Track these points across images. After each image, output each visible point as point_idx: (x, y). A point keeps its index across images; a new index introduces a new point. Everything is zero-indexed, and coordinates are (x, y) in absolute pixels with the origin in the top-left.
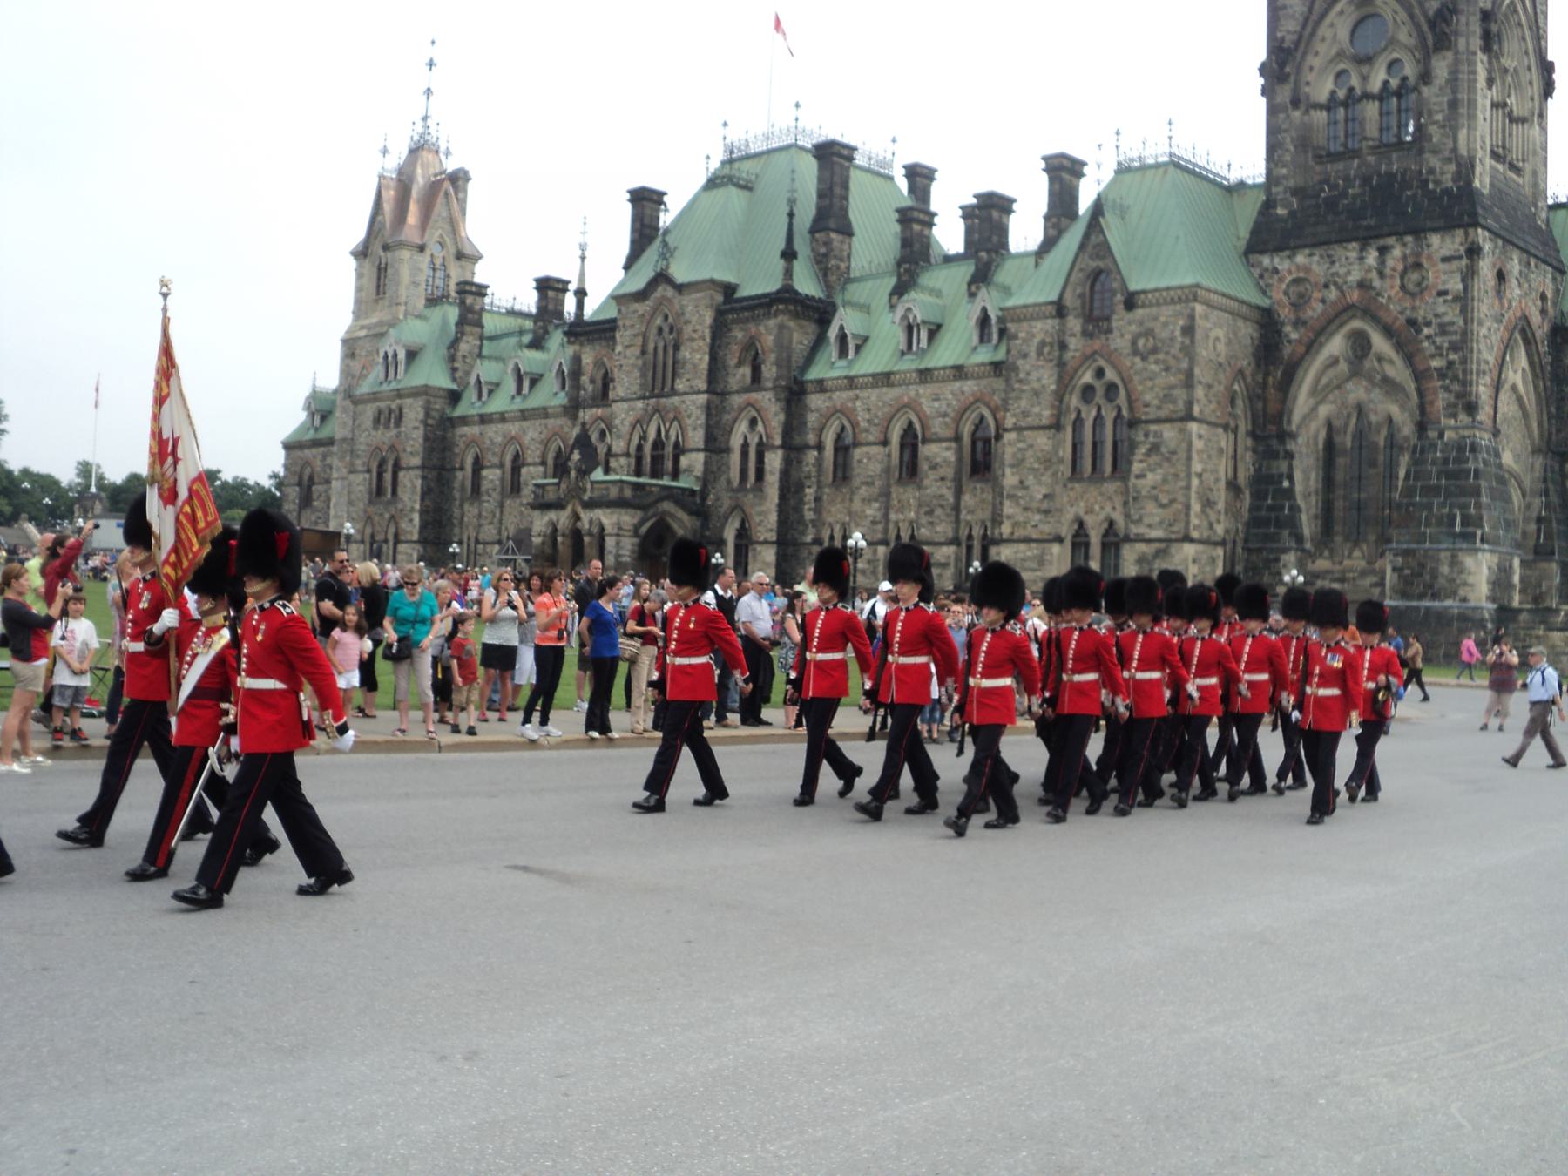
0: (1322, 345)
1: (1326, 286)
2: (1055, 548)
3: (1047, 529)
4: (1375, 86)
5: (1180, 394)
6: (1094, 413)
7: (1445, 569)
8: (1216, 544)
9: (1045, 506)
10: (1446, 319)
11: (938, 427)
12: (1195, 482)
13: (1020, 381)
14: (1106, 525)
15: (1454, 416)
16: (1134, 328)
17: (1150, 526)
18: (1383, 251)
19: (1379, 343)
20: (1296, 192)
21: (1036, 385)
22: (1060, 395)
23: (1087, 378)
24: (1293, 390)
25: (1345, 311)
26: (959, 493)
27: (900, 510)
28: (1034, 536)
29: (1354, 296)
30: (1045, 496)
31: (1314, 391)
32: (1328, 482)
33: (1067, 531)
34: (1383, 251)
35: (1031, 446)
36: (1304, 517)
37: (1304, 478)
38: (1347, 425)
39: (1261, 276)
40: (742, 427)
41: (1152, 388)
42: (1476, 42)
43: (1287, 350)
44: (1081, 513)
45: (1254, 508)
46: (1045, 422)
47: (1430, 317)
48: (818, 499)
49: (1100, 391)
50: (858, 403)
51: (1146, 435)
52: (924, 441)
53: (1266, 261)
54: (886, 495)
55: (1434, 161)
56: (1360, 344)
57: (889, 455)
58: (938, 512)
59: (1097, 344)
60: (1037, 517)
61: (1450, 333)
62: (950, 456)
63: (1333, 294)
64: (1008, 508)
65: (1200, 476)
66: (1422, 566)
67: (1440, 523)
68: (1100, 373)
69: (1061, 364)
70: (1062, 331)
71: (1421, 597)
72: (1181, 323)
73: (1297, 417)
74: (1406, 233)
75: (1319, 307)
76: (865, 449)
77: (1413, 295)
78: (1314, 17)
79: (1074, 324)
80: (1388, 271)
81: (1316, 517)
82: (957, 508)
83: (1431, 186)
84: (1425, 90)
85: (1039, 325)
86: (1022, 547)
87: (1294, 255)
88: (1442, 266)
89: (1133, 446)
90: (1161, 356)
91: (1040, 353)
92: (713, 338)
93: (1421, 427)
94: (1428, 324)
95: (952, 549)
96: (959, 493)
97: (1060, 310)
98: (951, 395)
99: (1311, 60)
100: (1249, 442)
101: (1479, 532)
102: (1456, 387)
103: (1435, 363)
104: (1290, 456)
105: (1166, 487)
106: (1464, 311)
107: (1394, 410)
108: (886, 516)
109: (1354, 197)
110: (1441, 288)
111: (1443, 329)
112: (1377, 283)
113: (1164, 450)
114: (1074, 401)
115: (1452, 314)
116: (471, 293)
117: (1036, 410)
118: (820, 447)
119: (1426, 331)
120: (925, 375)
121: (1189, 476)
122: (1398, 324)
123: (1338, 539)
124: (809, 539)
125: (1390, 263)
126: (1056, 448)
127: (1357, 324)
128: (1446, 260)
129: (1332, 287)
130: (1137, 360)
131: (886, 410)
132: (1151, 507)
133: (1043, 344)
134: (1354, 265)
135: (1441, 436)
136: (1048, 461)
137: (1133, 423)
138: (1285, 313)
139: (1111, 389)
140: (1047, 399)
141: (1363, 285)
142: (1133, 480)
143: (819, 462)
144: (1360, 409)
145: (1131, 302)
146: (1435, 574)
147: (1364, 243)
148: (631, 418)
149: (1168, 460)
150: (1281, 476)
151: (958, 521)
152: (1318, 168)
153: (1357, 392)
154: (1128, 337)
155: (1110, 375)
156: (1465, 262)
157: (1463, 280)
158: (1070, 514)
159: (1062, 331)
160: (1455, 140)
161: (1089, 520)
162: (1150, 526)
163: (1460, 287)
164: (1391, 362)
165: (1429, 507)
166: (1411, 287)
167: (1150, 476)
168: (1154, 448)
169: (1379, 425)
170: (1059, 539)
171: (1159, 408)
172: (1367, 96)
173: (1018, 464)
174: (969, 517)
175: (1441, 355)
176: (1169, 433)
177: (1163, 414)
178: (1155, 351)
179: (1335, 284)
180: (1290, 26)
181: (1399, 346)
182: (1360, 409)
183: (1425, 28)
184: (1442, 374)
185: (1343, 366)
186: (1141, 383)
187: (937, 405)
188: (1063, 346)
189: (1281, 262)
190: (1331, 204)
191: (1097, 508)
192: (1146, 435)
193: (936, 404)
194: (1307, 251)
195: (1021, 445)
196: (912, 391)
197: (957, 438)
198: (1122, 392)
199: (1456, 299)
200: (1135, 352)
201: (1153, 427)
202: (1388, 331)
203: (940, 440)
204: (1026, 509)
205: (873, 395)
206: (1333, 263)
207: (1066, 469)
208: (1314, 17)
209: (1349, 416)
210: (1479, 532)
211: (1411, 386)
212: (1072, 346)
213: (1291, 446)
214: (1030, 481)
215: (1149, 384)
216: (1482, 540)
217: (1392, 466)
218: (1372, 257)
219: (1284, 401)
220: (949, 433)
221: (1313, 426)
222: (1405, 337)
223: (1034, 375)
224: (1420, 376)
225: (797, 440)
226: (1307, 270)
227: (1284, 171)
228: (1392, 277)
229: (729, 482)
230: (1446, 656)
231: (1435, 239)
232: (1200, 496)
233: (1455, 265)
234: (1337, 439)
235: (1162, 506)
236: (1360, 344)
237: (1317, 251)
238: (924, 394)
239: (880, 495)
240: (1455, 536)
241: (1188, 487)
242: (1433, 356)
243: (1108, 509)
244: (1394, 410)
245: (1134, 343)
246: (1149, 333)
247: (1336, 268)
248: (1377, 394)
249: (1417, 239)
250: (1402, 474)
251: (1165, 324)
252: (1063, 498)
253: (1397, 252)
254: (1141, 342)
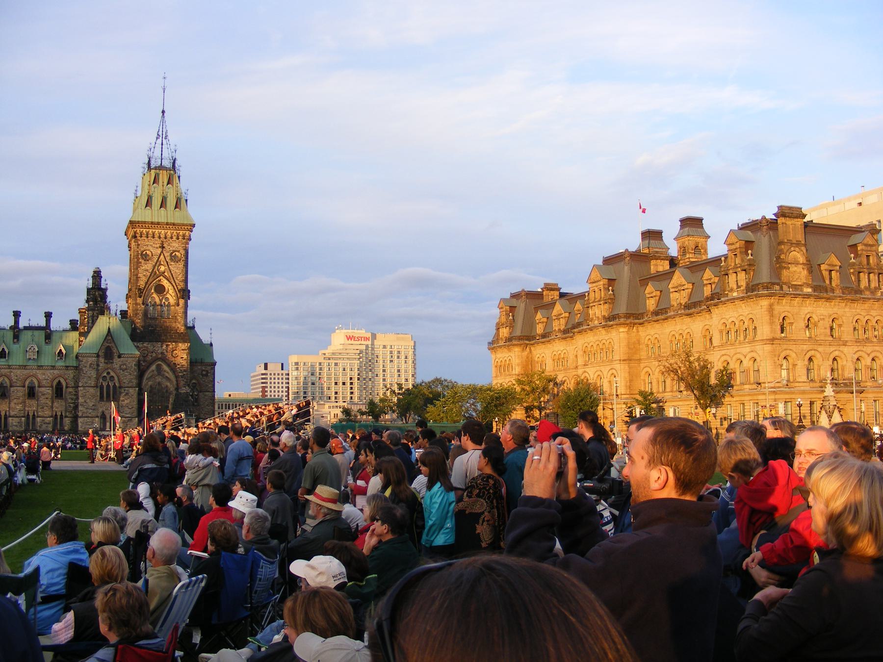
3: (94, 414)
11: (44, 383)
18: (167, 345)
19: (165, 367)
22: (97, 379)
25: (157, 359)
26: (53, 403)
27: (30, 406)
34: (167, 345)
52: (39, 387)
56: (159, 366)
59: (109, 366)
63: (154, 355)
64: (80, 408)
68: (108, 373)
69: (97, 370)
70: (98, 361)
79: (102, 360)
82: (52, 407)
89: (121, 393)
93: (177, 389)
96: (53, 403)
97: (98, 356)
98: (50, 374)
107: (168, 384)
120: (40, 367)
132: (126, 409)
136: (94, 396)
137: (120, 387)
141: (162, 353)
145: (119, 357)
153: (159, 379)
155: (112, 374)
158: (101, 410)
159: (98, 361)
168: (127, 394)
173: (83, 396)
177: (130, 385)
182: (159, 384)
184: (182, 377)
185: (156, 372)
187: (45, 376)
188: (98, 365)
196: (34, 371)
197: (52, 387)
202: (169, 365)
205: (19, 372)
218: (165, 346)
223: (89, 372)
224: (177, 377)
236: (159, 366)
238: (39, 374)
244: (168, 384)
248: (164, 380)
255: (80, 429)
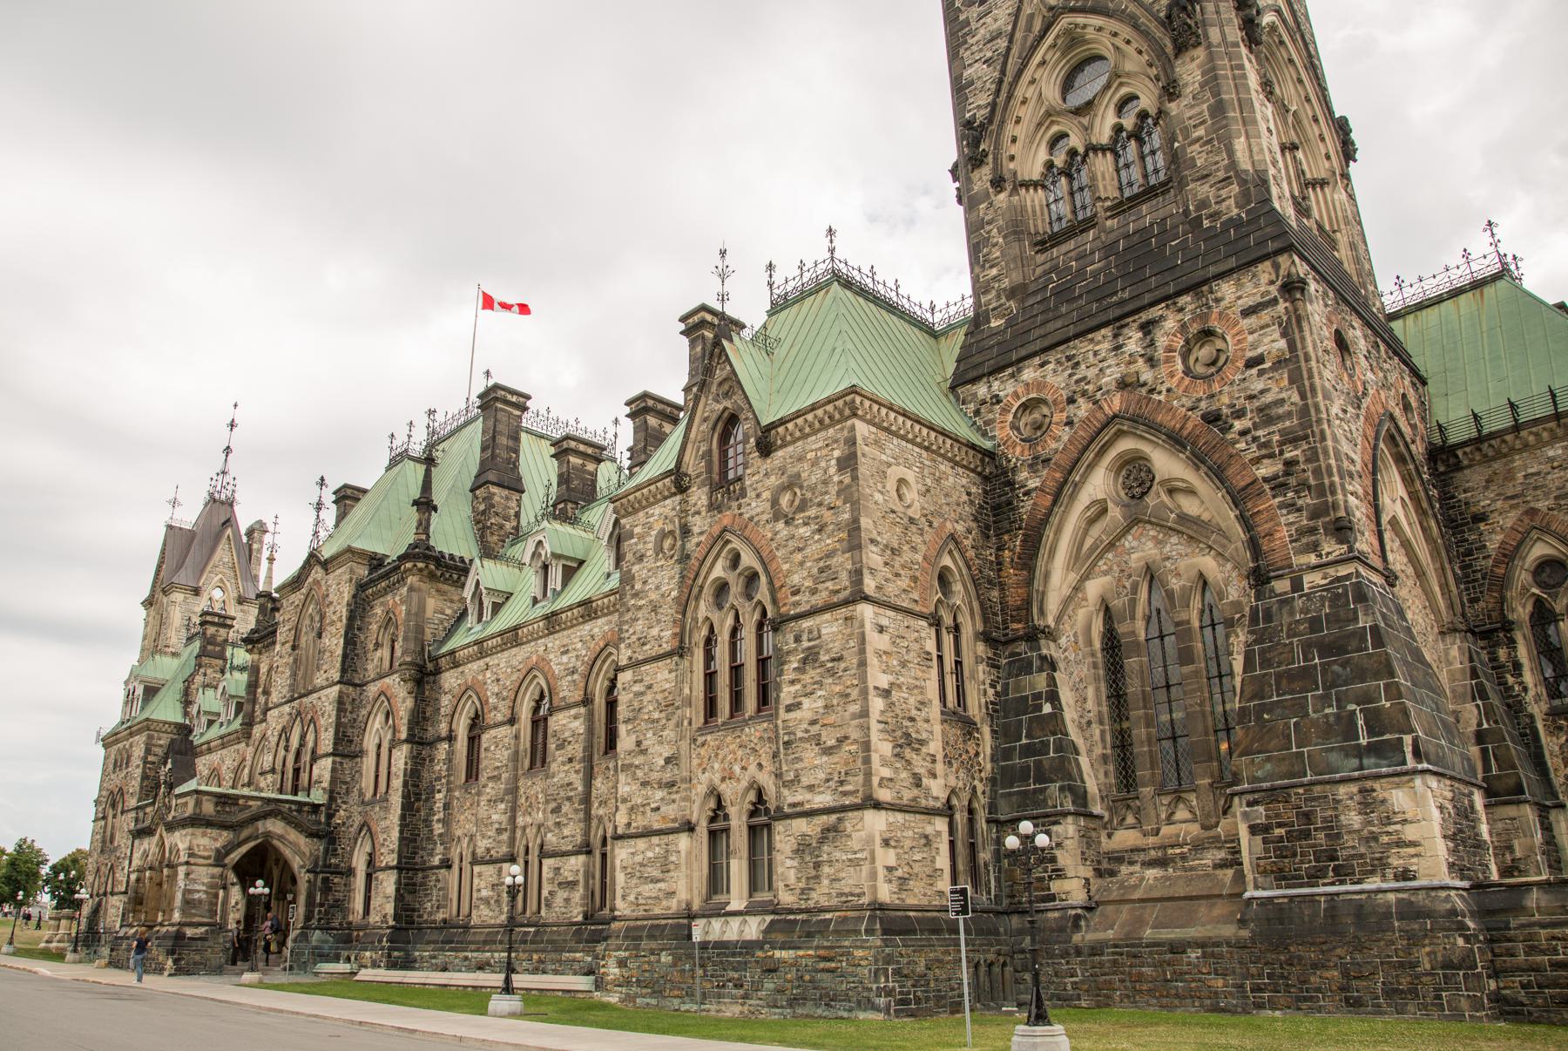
0: (1077, 487)
1: (1071, 401)
2: (683, 841)
4: (1103, 134)
5: (843, 562)
6: (730, 621)
7: (1353, 819)
8: (931, 812)
9: (667, 776)
10: (1268, 398)
12: (877, 704)
13: (636, 595)
14: (752, 796)
15: (1314, 548)
16: (773, 481)
17: (811, 788)
18: (1147, 328)
19: (1166, 464)
20: (1012, 293)
21: (653, 596)
22: (684, 605)
23: (719, 571)
24: (1041, 563)
28: (656, 826)
29: (1116, 403)
30: (668, 761)
31: (1076, 557)
32: (1117, 698)
33: (699, 813)
34: (1147, 328)
35: (650, 687)
36: (1084, 761)
37: (1078, 699)
38: (1133, 602)
39: (977, 413)
40: (377, 722)
41: (802, 564)
42: (1235, 33)
43: (1026, 507)
44: (717, 781)
45: (999, 755)
46: (667, 647)
47: (1240, 403)
48: (447, 806)
49: (736, 588)
50: (488, 674)
51: (797, 639)
53: (981, 390)
54: (513, 791)
55: (1204, 190)
56: (1137, 477)
57: (517, 737)
58: (566, 808)
59: (726, 518)
60: (659, 794)
61: (1280, 418)
62: (579, 726)
65: (886, 693)
66: (1307, 817)
67: (1327, 731)
68: (735, 560)
69: (685, 558)
71: (1315, 877)
72: (837, 453)
73: (1053, 604)
74: (1179, 294)
75: (1065, 434)
76: (493, 732)
77: (1206, 378)
78: (1008, 79)
79: (699, 496)
80: (1160, 353)
81: (1105, 758)
82: (587, 799)
83: (1206, 223)
84: (1173, 108)
85: (656, 510)
86: (641, 844)
87: (1020, 371)
88: (1246, 323)
90: (812, 512)
91: (659, 549)
92: (351, 618)
93: (1259, 578)
94: (1240, 414)
95: (582, 858)
99: (1010, 129)
100: (981, 648)
101: (1408, 739)
102: (1307, 500)
103: (1265, 470)
104: (1050, 665)
105: (831, 719)
106: (1295, 379)
107: (1208, 563)
108: (513, 819)
109: (1095, 274)
110: (1250, 354)
111: (1266, 416)
112: (1147, 375)
113: (824, 657)
114: (704, 609)
115: (1276, 388)
116: (213, 624)
117: (655, 632)
118: (451, 738)
119: (1238, 425)
121: (864, 693)
122: (1190, 425)
123: (1146, 791)
124: (436, 861)
125: (1162, 342)
126: (680, 682)
127: (1126, 445)
128: (1248, 312)
129: (1081, 401)
130: (781, 525)
131: (514, 677)
132: (810, 755)
133: (663, 535)
134: (1104, 361)
135: (1297, 585)
138: (1017, 454)
139: (752, 578)
140: (668, 611)
142: (782, 714)
143: (449, 760)
144: (1151, 574)
146: (1334, 834)
147: (1117, 324)
148: (279, 727)
149: (832, 673)
150: (1038, 696)
151: (588, 817)
152: (1040, 258)
153: (1142, 548)
154: (766, 495)
156: (1282, 306)
157: (1284, 335)
160: (1231, 153)
161: (728, 790)
162: (811, 788)
163: (1282, 344)
164: (1191, 492)
165: (1300, 708)
166: (1200, 369)
167: (806, 703)
168: (810, 658)
169: (1186, 594)
170: (690, 828)
171: (814, 592)
172: (1093, 148)
174: (601, 812)
175: (1271, 456)
176: (829, 627)
177: (819, 599)
178: (803, 507)
179: (1084, 393)
180: (979, 102)
181: (1198, 459)
182: (1151, 574)
183: (1158, 33)
184: (1278, 486)
185: (1115, 513)
186: (786, 560)
188: (686, 531)
189: (1004, 387)
190: (1064, 294)
191: (737, 769)
192: (797, 639)
193: (565, 659)
194: (1037, 361)
195: (637, 688)
197: (587, 701)
198: (763, 579)
199: (1279, 363)
200: (777, 515)
201: (806, 624)
202: (1176, 441)
203: (569, 707)
204: (644, 784)
206: (1078, 364)
207: (697, 714)
208: (1008, 79)
209: (1135, 589)
210: (1408, 739)
211: (1228, 517)
212: (696, 530)
213: (1048, 649)
214: (650, 740)
215: (799, 557)
216: (1417, 754)
217: (1219, 656)
218: (1133, 341)
219: (1029, 582)
220: (577, 696)
221: (1081, 614)
222: (1205, 441)
224: (1238, 498)
225: (431, 733)
226: (1040, 385)
227: (994, 272)
228: (1168, 360)
229: (361, 794)
230: (1391, 992)
231: (1226, 289)
232: (888, 730)
233: (1266, 316)
234: (1122, 629)
235: (828, 751)
236: (1137, 477)
237: (1052, 357)
239: (507, 792)
240: (1360, 753)
241: (865, 713)
242: (1257, 461)
243: (753, 768)
244: (1208, 563)
245: (775, 502)
246: (792, 484)
247: (1082, 371)
248: (1174, 545)
249: (1199, 296)
250: (1238, 665)
251: (815, 463)
252: (692, 759)
253: (1170, 324)
254: (785, 500)
255: (622, 907)
